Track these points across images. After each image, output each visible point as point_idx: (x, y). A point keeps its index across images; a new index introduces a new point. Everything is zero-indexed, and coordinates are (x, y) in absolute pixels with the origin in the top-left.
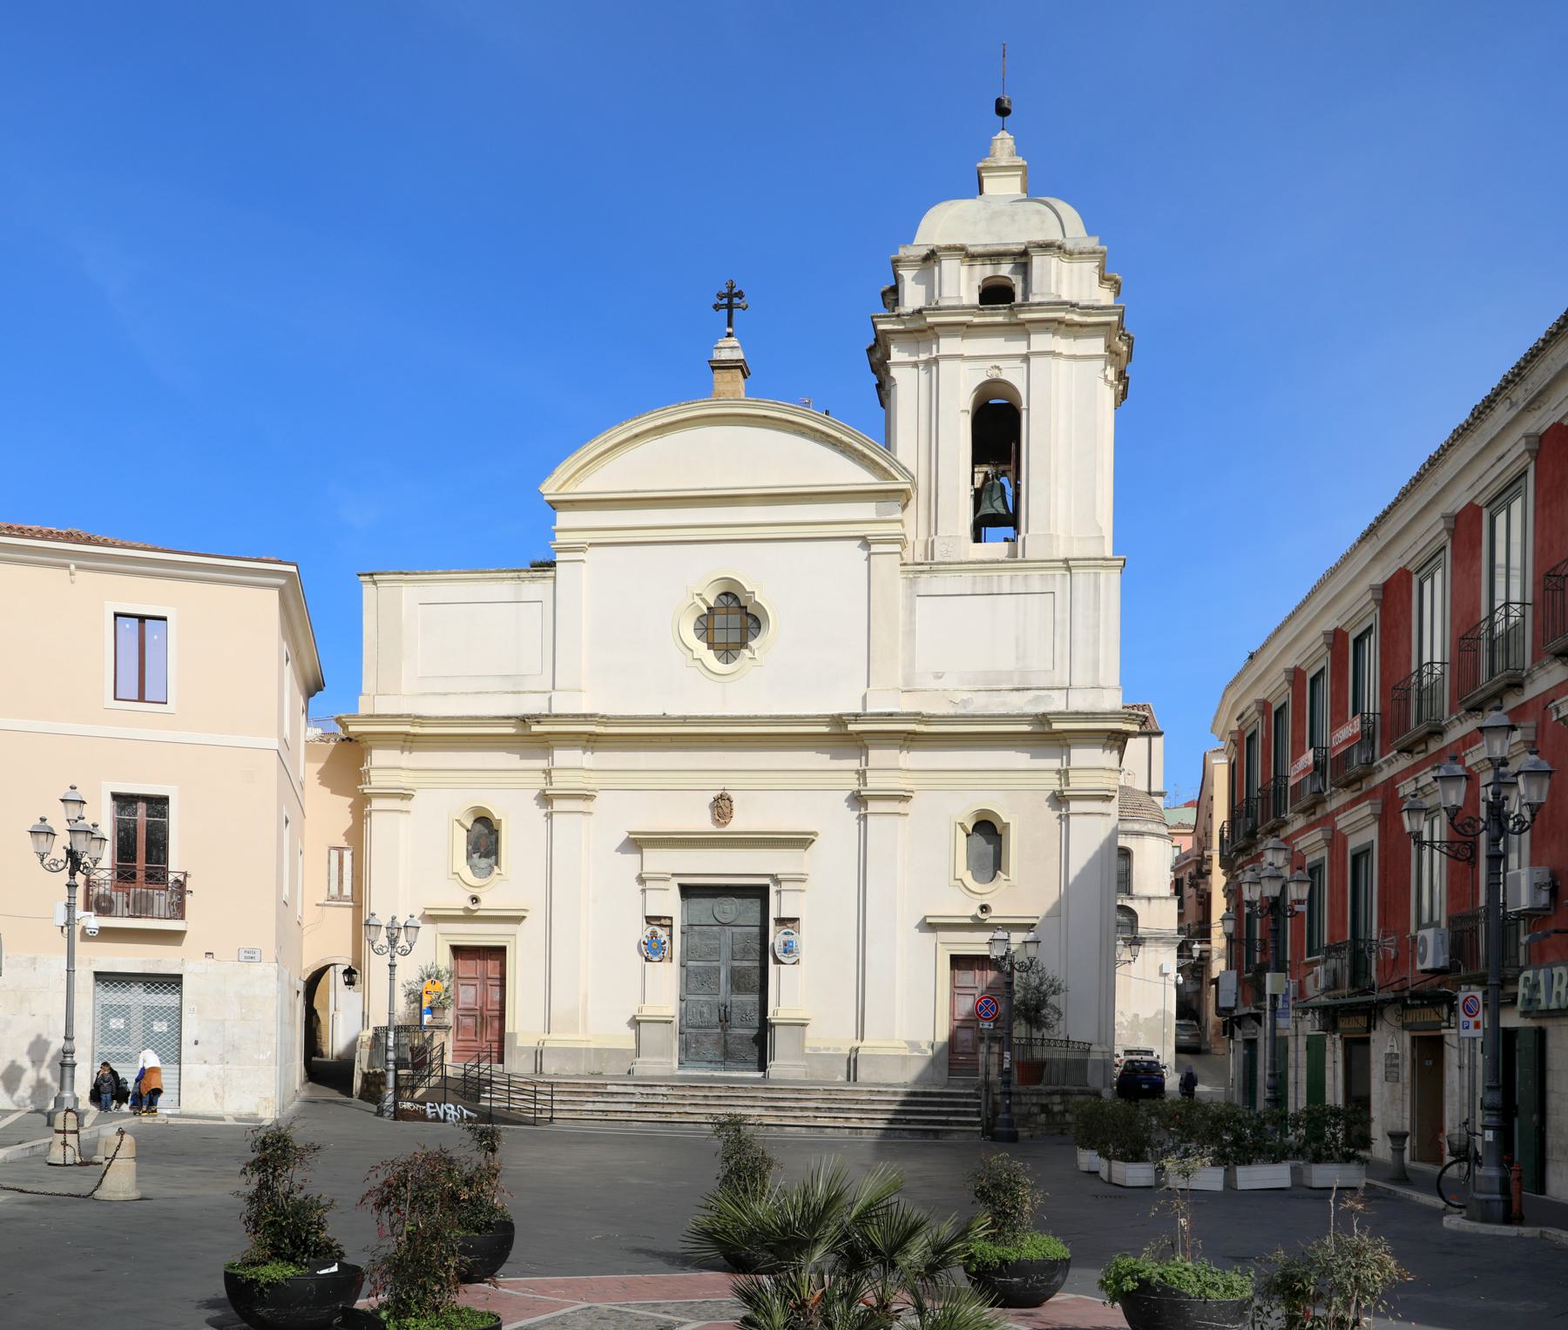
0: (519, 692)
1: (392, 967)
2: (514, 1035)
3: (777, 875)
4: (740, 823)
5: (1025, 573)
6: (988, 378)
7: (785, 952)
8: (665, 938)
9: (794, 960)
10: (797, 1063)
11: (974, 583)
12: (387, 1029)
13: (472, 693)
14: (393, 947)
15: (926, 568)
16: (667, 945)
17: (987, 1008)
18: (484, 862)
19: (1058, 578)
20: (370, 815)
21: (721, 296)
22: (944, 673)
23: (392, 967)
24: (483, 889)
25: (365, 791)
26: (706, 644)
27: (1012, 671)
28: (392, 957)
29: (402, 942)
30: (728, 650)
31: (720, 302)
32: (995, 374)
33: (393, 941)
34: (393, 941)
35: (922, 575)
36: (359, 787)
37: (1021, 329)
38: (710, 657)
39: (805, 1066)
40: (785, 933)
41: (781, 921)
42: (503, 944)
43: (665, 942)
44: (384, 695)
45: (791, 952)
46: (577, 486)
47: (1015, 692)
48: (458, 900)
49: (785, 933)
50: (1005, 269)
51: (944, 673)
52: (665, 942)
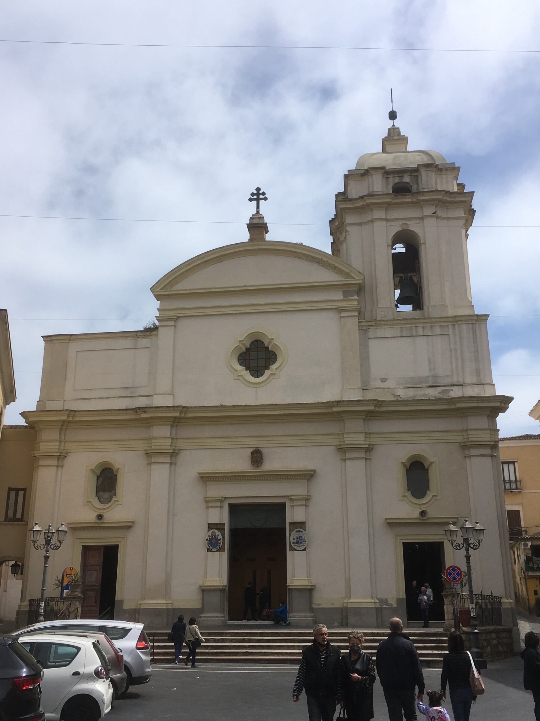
0: (134, 397)
1: (47, 558)
2: (121, 602)
3: (291, 496)
4: (268, 466)
6: (401, 229)
7: (297, 542)
8: (220, 536)
9: (303, 547)
10: (306, 615)
11: (402, 331)
12: (39, 601)
13: (105, 398)
14: (48, 546)
15: (374, 323)
16: (221, 541)
17: (454, 574)
18: (107, 495)
19: (450, 327)
20: (38, 467)
21: (253, 194)
23: (47, 558)
24: (105, 511)
25: (36, 455)
27: (428, 377)
28: (47, 551)
29: (53, 542)
30: (257, 371)
31: (252, 198)
32: (405, 227)
33: (48, 542)
34: (48, 542)
35: (371, 328)
36: (32, 453)
37: (419, 204)
38: (247, 374)
40: (297, 532)
41: (294, 525)
42: (117, 544)
43: (220, 539)
44: (52, 400)
45: (301, 543)
46: (171, 288)
47: (430, 388)
48: (90, 517)
49: (297, 532)
50: (407, 179)
51: (387, 379)
52: (220, 539)
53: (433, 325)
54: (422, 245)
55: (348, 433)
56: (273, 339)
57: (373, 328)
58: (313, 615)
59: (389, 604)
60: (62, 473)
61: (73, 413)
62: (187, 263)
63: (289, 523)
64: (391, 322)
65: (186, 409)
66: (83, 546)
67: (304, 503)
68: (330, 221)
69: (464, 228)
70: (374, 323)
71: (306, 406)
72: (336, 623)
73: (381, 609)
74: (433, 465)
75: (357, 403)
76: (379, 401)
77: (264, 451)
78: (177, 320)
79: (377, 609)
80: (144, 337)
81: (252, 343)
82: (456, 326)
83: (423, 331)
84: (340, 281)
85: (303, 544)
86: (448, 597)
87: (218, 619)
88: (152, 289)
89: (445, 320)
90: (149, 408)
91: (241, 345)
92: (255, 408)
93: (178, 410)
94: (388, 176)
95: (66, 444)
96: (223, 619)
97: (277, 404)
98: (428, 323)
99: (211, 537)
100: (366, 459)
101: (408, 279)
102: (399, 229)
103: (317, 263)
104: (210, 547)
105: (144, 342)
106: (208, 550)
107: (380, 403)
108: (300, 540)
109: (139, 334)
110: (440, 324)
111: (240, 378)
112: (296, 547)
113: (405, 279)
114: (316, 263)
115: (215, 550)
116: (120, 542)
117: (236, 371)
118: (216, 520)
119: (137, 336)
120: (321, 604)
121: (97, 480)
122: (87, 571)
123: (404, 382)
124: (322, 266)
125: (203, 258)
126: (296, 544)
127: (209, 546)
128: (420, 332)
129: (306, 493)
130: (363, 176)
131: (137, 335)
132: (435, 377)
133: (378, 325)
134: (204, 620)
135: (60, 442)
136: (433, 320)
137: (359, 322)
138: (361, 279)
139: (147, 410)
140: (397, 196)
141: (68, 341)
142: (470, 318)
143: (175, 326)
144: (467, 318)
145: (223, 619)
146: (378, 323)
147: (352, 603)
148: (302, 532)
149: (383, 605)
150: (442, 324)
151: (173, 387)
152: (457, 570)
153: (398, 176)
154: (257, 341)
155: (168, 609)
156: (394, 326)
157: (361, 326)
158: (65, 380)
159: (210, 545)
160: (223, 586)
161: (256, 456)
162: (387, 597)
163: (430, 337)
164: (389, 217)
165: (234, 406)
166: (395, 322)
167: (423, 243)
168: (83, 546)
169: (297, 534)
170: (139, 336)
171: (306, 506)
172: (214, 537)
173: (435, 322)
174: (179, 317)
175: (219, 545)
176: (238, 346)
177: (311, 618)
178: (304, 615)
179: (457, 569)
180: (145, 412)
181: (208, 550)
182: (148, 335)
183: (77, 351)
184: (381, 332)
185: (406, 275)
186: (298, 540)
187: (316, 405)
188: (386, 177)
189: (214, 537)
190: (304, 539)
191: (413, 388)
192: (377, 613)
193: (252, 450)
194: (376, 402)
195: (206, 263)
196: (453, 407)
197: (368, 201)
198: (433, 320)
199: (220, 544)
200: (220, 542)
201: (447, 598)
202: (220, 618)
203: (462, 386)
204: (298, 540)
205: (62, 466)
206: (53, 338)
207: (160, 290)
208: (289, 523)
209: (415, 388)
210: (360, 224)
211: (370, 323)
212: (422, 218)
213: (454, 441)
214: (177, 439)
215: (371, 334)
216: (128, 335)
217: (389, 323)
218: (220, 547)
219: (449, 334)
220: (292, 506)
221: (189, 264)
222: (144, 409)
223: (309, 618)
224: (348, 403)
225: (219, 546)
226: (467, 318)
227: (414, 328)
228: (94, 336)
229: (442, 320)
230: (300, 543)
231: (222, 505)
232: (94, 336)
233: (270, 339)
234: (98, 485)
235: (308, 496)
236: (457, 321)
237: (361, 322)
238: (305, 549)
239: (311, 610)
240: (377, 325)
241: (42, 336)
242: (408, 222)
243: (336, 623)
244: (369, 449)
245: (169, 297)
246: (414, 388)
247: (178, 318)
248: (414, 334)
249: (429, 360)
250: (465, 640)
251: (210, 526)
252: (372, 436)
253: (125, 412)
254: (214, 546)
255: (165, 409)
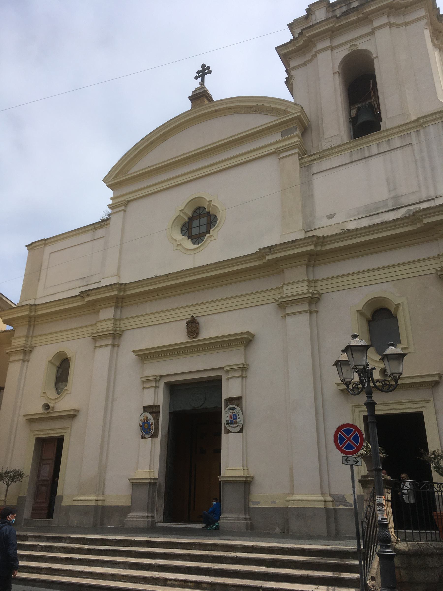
2: (61, 497)
5: (386, 139)
6: (350, 52)
7: (232, 422)
8: (152, 421)
9: (239, 428)
10: (239, 516)
16: (153, 425)
22: (335, 214)
26: (186, 237)
27: (387, 200)
32: (353, 48)
38: (189, 244)
39: (246, 519)
40: (230, 409)
41: (230, 401)
42: (62, 434)
43: (152, 424)
45: (236, 423)
47: (390, 212)
49: (230, 409)
51: (335, 214)
53: (390, 138)
54: (375, 60)
55: (286, 284)
56: (211, 201)
57: (317, 161)
58: (248, 516)
59: (348, 504)
60: (27, 367)
61: (33, 307)
62: (134, 149)
63: (225, 399)
64: (337, 150)
65: (123, 286)
66: (36, 438)
67: (239, 374)
68: (285, 82)
69: (428, 28)
70: (317, 156)
71: (238, 261)
72: (277, 528)
73: (335, 510)
74: (401, 307)
75: (293, 244)
76: (318, 238)
77: (199, 320)
78: (127, 205)
79: (327, 510)
80: (101, 227)
81: (195, 211)
82: (422, 132)
83: (378, 148)
84: (275, 121)
85: (238, 424)
86: (368, 485)
87: (143, 519)
88: (105, 180)
89: (404, 128)
90: (91, 291)
91: (182, 215)
92: (188, 272)
93: (115, 288)
94: (335, 8)
95: (34, 339)
96: (149, 519)
97: (208, 264)
98: (382, 138)
99: (143, 422)
100: (311, 312)
101: (367, 106)
102: (347, 52)
103: (255, 112)
104: (144, 433)
105: (100, 232)
106: (143, 437)
107: (322, 240)
108: (234, 419)
109: (97, 226)
110: (400, 135)
111: (180, 247)
112: (230, 429)
113: (363, 108)
114: (253, 112)
115: (148, 436)
116: (65, 432)
117: (176, 240)
118: (150, 403)
119: (95, 228)
120: (259, 502)
121: (58, 371)
122: (42, 465)
123: (356, 213)
124: (259, 113)
125: (148, 140)
126: (230, 425)
127: (142, 433)
128: (374, 150)
129: (242, 361)
130: (307, 19)
131: (96, 227)
132: (396, 198)
133: (322, 157)
134: (129, 520)
135: (27, 337)
136: (391, 132)
137: (300, 159)
138: (299, 110)
139: (89, 293)
140: (340, 18)
141: (43, 246)
142: (438, 116)
143: (125, 211)
144: (434, 117)
145: (149, 519)
146: (322, 154)
147: (294, 500)
148: (236, 409)
149: (339, 505)
150: (402, 134)
151: (119, 268)
152: (355, 432)
153: (345, 5)
154: (199, 208)
155: (96, 507)
156: (342, 153)
157: (304, 163)
158: (39, 281)
159: (142, 431)
160: (151, 479)
161: (191, 326)
162: (344, 494)
163: (388, 155)
164: (334, 44)
165: (166, 275)
166: (342, 148)
167: (375, 58)
168: (36, 438)
169: (230, 412)
170: (97, 227)
171: (243, 377)
172: (146, 421)
173: (394, 134)
174: (129, 202)
175: (151, 430)
176: (179, 215)
177: (244, 522)
178: (236, 516)
179: (354, 430)
180: (88, 295)
181: (143, 437)
182: (104, 225)
183: (50, 253)
184: (326, 164)
185: (364, 104)
186: (232, 419)
187: (248, 258)
188: (332, 11)
189: (146, 421)
190: (239, 418)
191: (368, 216)
192: (328, 518)
193: (187, 320)
194: (315, 239)
195: (153, 144)
196: (419, 225)
197: (307, 35)
198: (391, 132)
199: (152, 429)
200: (153, 427)
201: (365, 488)
202: (145, 518)
203: (434, 200)
204: (232, 419)
205: (28, 361)
206: (33, 245)
207: (112, 179)
208: (225, 399)
209: (369, 216)
210: (305, 64)
211: (313, 158)
212: (372, 33)
213: (429, 272)
214: (120, 320)
215: (315, 169)
216: (88, 229)
217: (335, 151)
218: (153, 433)
219: (412, 143)
220: (228, 379)
221: (136, 149)
222: (87, 293)
223: (242, 521)
224: (282, 247)
225: (152, 432)
226: (434, 117)
227: (366, 149)
228: (63, 236)
229: (401, 129)
230: (235, 423)
231: (157, 384)
232: (63, 236)
233: (209, 201)
234: (58, 377)
235: (243, 364)
236: (421, 125)
237: (302, 158)
238: (241, 431)
239: (247, 509)
240: (320, 158)
241: (26, 246)
242: (356, 43)
243: (277, 528)
244: (314, 299)
245: (120, 185)
246: (369, 217)
247: (127, 203)
248: (367, 155)
249: (388, 180)
250: (399, 568)
251: (146, 409)
252: (319, 284)
253: (74, 299)
254: (147, 433)
255: (104, 289)
